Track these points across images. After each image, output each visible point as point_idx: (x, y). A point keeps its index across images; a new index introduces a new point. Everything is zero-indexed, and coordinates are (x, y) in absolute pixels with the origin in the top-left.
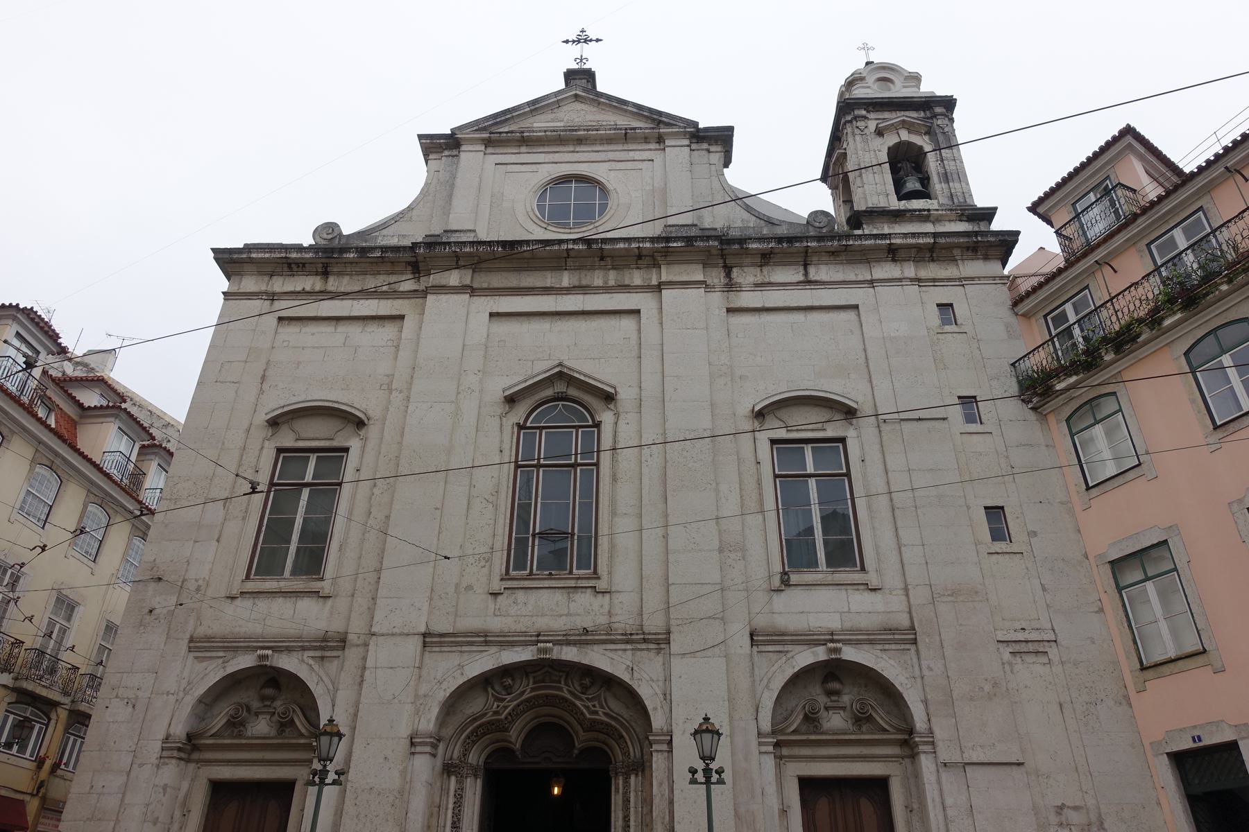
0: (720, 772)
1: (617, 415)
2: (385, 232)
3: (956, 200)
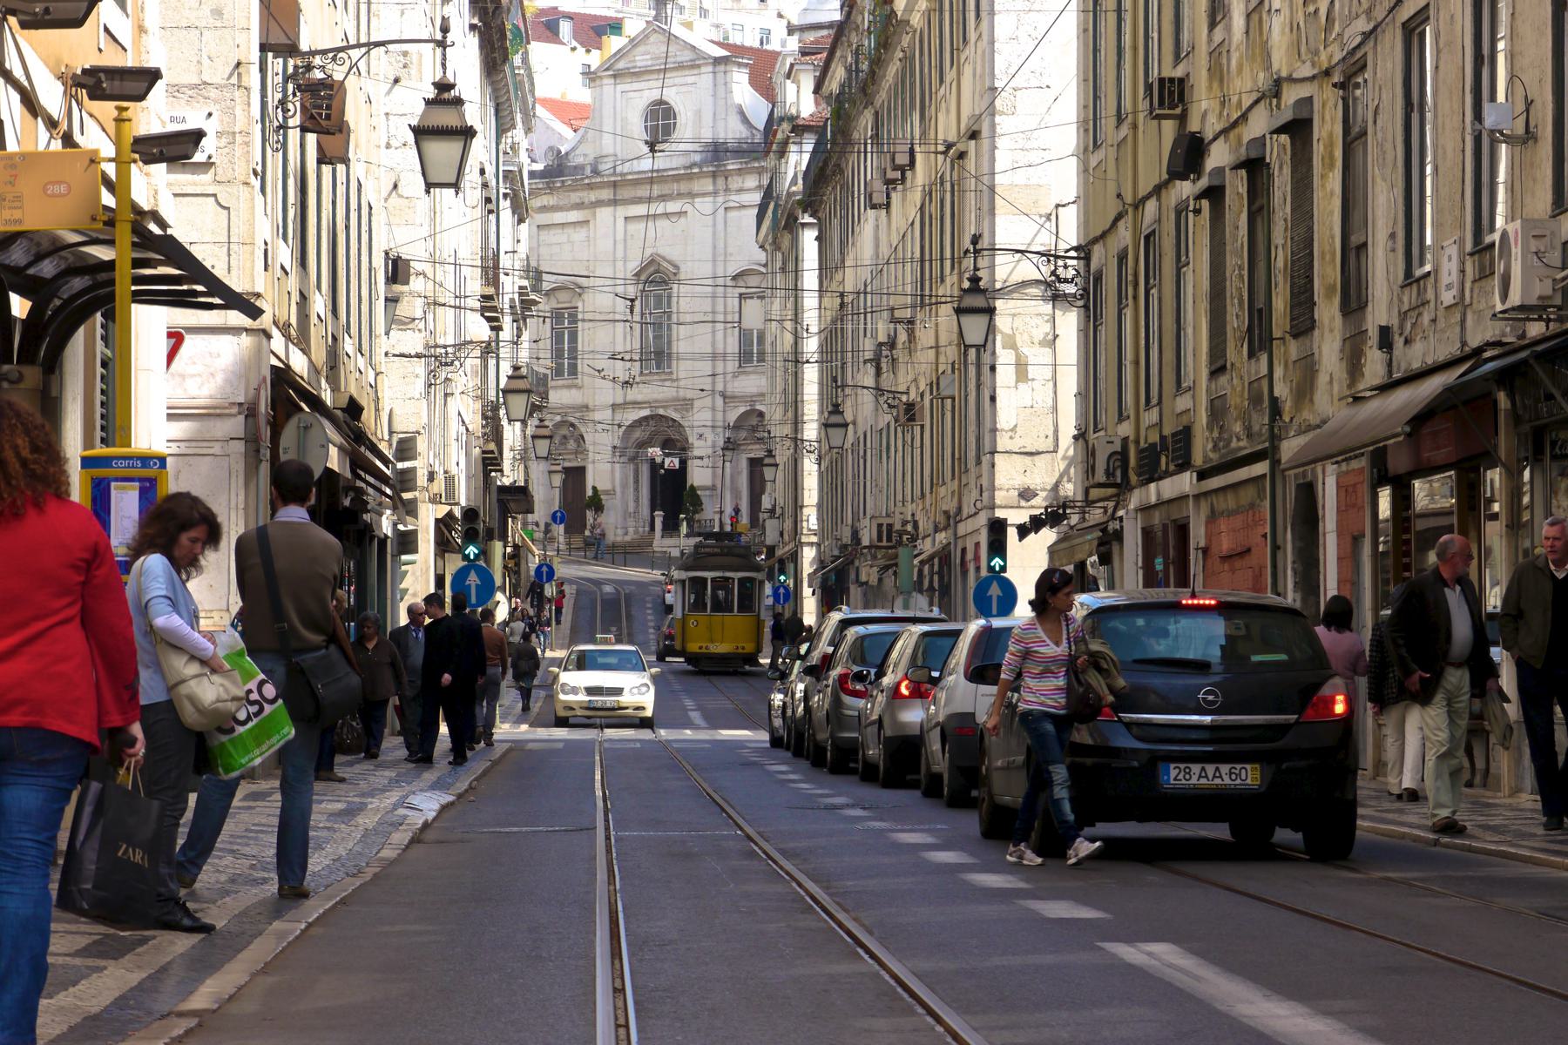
2: (577, 152)
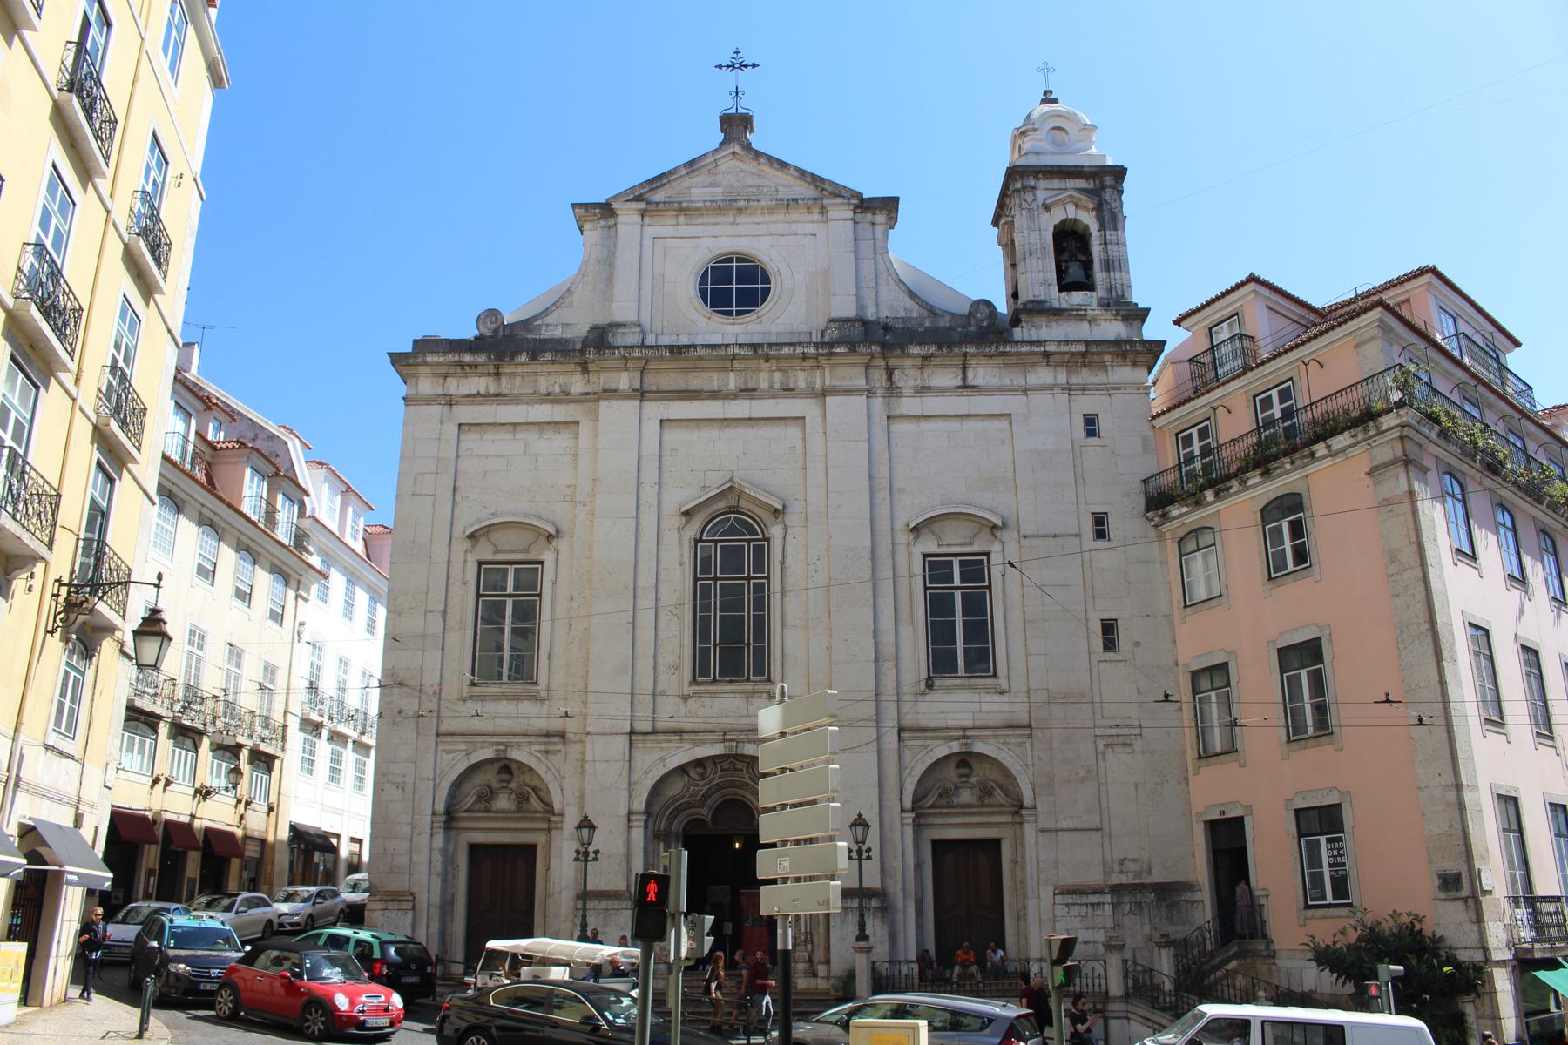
0: (869, 850)
1: (786, 529)
2: (548, 320)
3: (1114, 294)
